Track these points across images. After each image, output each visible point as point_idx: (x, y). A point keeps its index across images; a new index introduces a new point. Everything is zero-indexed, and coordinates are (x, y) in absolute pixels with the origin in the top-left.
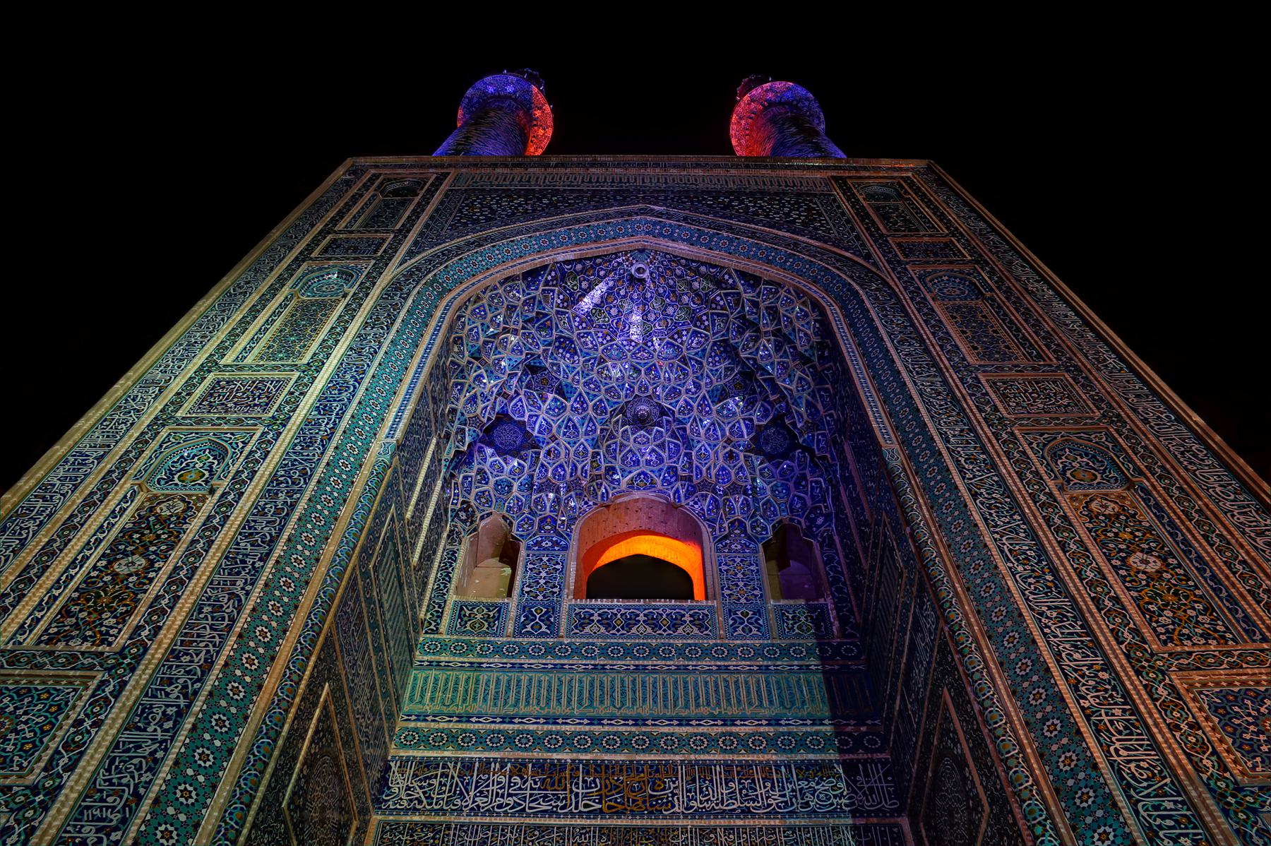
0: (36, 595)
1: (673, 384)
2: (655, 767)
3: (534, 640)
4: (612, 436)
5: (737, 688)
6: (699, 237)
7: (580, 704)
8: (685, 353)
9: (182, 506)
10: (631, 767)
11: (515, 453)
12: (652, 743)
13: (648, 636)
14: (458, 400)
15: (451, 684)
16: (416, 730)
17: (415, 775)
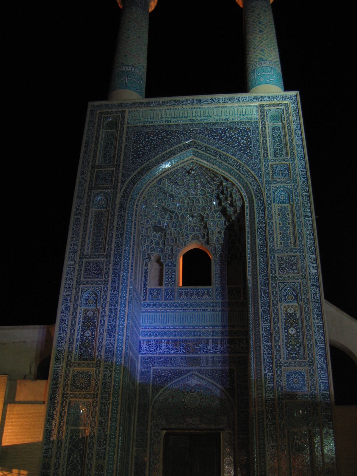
1: (204, 205)
2: (197, 341)
3: (169, 301)
4: (186, 224)
5: (216, 316)
6: (210, 160)
7: (181, 322)
8: (207, 195)
9: (92, 314)
10: (192, 341)
11: (160, 231)
12: (196, 334)
13: (196, 299)
14: (142, 231)
15: (151, 317)
16: (145, 331)
17: (146, 344)
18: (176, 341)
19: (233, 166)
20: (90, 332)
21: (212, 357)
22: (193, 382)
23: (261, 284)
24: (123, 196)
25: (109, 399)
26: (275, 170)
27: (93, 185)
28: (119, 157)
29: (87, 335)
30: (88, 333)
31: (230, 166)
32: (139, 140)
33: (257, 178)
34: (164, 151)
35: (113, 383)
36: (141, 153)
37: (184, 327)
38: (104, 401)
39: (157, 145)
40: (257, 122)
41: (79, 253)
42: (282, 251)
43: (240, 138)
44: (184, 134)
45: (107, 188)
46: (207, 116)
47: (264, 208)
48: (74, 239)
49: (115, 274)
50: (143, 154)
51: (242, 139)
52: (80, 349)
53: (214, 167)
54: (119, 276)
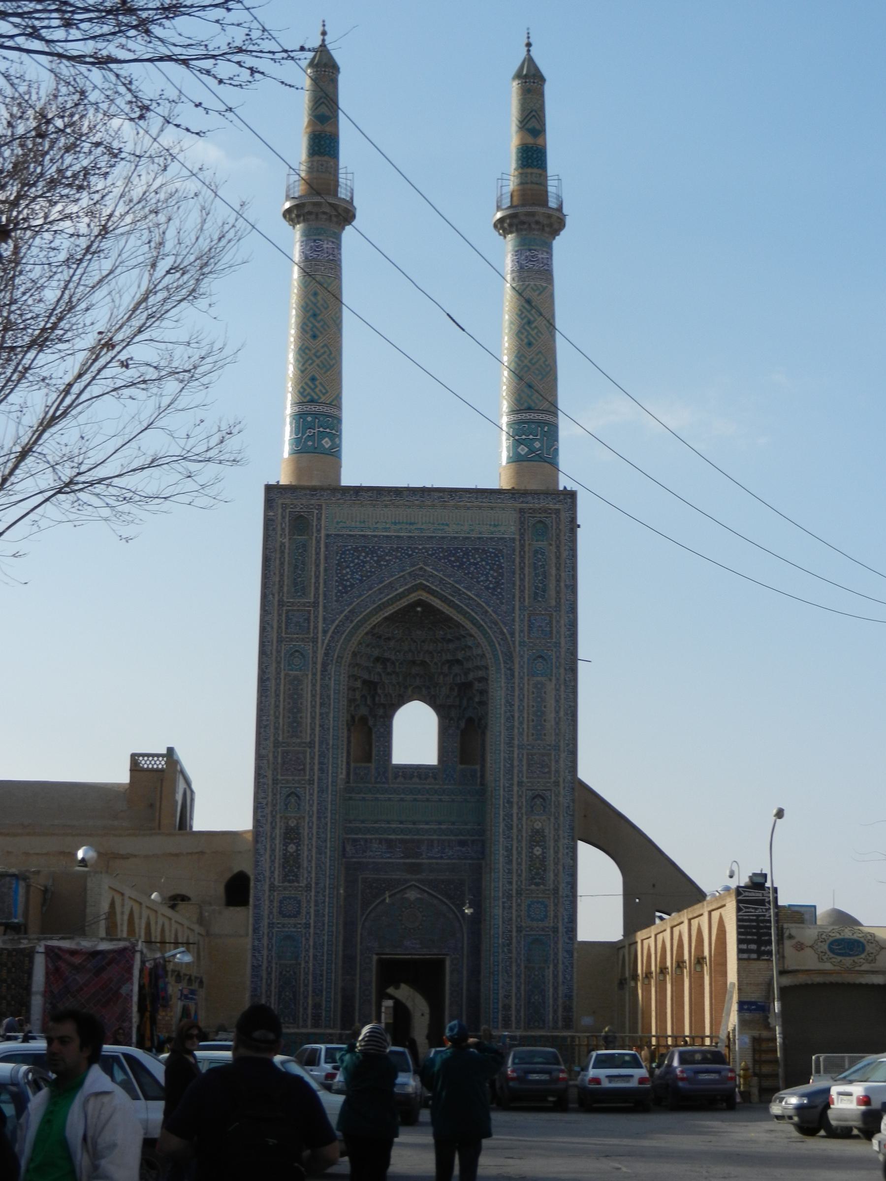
0: (277, 865)
9: (295, 822)
18: (391, 840)
19: (476, 613)
20: (294, 847)
21: (437, 864)
22: (412, 895)
23: (504, 790)
24: (326, 654)
25: (324, 930)
26: (533, 624)
27: (283, 635)
28: (317, 589)
29: (291, 851)
30: (292, 848)
31: (473, 614)
32: (345, 561)
33: (508, 636)
34: (381, 582)
35: (327, 910)
36: (348, 583)
37: (401, 823)
38: (318, 931)
39: (370, 572)
40: (514, 539)
41: (272, 739)
42: (533, 747)
43: (488, 567)
44: (410, 556)
45: (303, 640)
46: (443, 524)
47: (514, 683)
48: (264, 718)
49: (321, 770)
50: (352, 586)
51: (491, 569)
52: (284, 867)
53: (451, 610)
54: (328, 773)
